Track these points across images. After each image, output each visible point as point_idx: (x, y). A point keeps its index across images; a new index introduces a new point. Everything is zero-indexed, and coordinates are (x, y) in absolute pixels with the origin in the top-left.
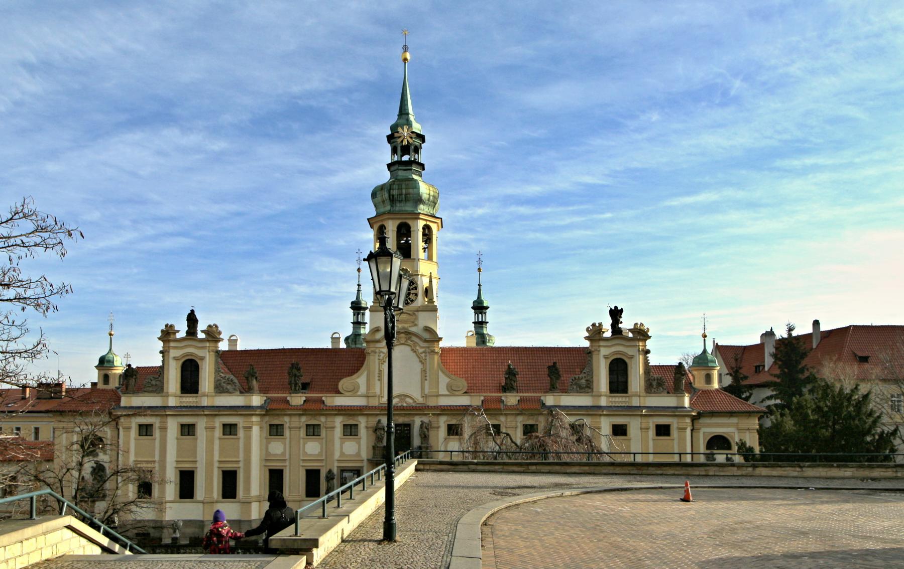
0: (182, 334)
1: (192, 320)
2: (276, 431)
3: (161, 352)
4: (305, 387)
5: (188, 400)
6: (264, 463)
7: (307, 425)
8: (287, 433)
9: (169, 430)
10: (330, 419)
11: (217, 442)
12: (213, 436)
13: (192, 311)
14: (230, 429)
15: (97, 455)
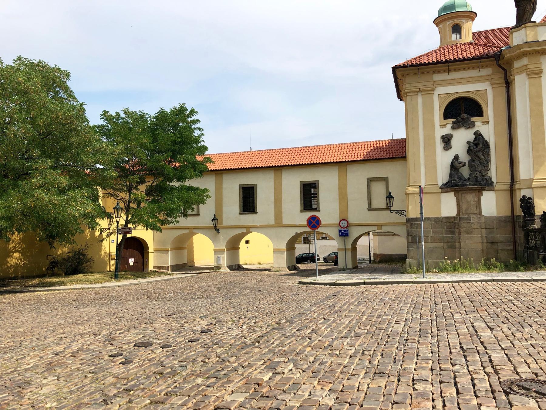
15: (473, 125)
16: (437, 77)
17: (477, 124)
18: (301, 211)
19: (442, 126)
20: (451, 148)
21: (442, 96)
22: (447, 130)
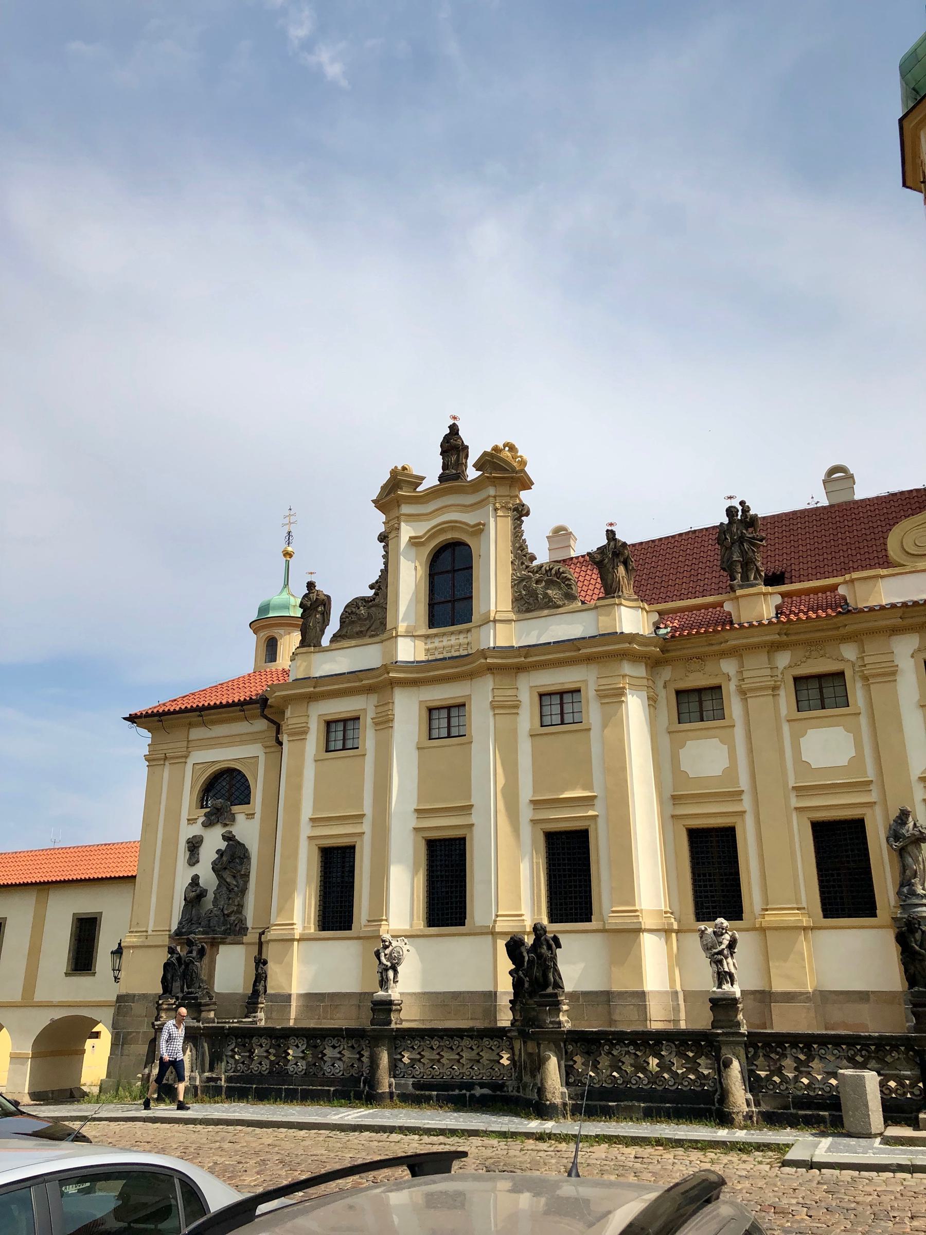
0: (431, 480)
1: (453, 447)
2: (696, 705)
3: (383, 538)
4: (773, 580)
5: (446, 642)
6: (670, 810)
7: (797, 680)
8: (734, 707)
9: (396, 724)
10: (871, 647)
11: (525, 747)
12: (514, 731)
13: (454, 429)
14: (559, 706)
16: (197, 733)
17: (240, 818)
18: (67, 974)
19: (191, 821)
20: (198, 862)
21: (198, 767)
22: (196, 829)
